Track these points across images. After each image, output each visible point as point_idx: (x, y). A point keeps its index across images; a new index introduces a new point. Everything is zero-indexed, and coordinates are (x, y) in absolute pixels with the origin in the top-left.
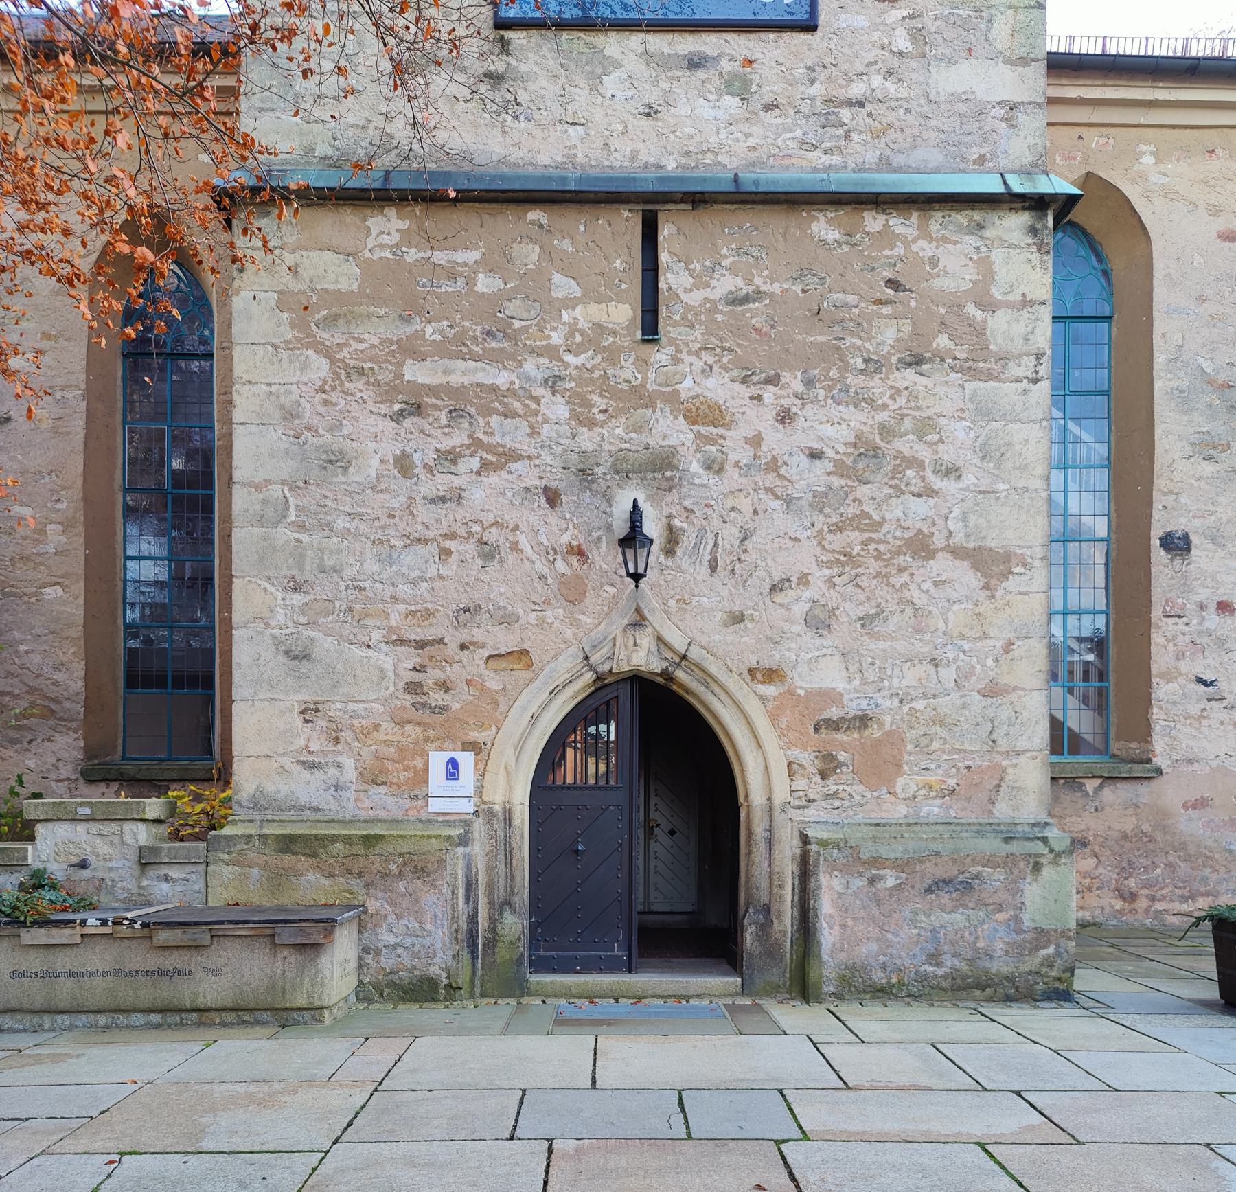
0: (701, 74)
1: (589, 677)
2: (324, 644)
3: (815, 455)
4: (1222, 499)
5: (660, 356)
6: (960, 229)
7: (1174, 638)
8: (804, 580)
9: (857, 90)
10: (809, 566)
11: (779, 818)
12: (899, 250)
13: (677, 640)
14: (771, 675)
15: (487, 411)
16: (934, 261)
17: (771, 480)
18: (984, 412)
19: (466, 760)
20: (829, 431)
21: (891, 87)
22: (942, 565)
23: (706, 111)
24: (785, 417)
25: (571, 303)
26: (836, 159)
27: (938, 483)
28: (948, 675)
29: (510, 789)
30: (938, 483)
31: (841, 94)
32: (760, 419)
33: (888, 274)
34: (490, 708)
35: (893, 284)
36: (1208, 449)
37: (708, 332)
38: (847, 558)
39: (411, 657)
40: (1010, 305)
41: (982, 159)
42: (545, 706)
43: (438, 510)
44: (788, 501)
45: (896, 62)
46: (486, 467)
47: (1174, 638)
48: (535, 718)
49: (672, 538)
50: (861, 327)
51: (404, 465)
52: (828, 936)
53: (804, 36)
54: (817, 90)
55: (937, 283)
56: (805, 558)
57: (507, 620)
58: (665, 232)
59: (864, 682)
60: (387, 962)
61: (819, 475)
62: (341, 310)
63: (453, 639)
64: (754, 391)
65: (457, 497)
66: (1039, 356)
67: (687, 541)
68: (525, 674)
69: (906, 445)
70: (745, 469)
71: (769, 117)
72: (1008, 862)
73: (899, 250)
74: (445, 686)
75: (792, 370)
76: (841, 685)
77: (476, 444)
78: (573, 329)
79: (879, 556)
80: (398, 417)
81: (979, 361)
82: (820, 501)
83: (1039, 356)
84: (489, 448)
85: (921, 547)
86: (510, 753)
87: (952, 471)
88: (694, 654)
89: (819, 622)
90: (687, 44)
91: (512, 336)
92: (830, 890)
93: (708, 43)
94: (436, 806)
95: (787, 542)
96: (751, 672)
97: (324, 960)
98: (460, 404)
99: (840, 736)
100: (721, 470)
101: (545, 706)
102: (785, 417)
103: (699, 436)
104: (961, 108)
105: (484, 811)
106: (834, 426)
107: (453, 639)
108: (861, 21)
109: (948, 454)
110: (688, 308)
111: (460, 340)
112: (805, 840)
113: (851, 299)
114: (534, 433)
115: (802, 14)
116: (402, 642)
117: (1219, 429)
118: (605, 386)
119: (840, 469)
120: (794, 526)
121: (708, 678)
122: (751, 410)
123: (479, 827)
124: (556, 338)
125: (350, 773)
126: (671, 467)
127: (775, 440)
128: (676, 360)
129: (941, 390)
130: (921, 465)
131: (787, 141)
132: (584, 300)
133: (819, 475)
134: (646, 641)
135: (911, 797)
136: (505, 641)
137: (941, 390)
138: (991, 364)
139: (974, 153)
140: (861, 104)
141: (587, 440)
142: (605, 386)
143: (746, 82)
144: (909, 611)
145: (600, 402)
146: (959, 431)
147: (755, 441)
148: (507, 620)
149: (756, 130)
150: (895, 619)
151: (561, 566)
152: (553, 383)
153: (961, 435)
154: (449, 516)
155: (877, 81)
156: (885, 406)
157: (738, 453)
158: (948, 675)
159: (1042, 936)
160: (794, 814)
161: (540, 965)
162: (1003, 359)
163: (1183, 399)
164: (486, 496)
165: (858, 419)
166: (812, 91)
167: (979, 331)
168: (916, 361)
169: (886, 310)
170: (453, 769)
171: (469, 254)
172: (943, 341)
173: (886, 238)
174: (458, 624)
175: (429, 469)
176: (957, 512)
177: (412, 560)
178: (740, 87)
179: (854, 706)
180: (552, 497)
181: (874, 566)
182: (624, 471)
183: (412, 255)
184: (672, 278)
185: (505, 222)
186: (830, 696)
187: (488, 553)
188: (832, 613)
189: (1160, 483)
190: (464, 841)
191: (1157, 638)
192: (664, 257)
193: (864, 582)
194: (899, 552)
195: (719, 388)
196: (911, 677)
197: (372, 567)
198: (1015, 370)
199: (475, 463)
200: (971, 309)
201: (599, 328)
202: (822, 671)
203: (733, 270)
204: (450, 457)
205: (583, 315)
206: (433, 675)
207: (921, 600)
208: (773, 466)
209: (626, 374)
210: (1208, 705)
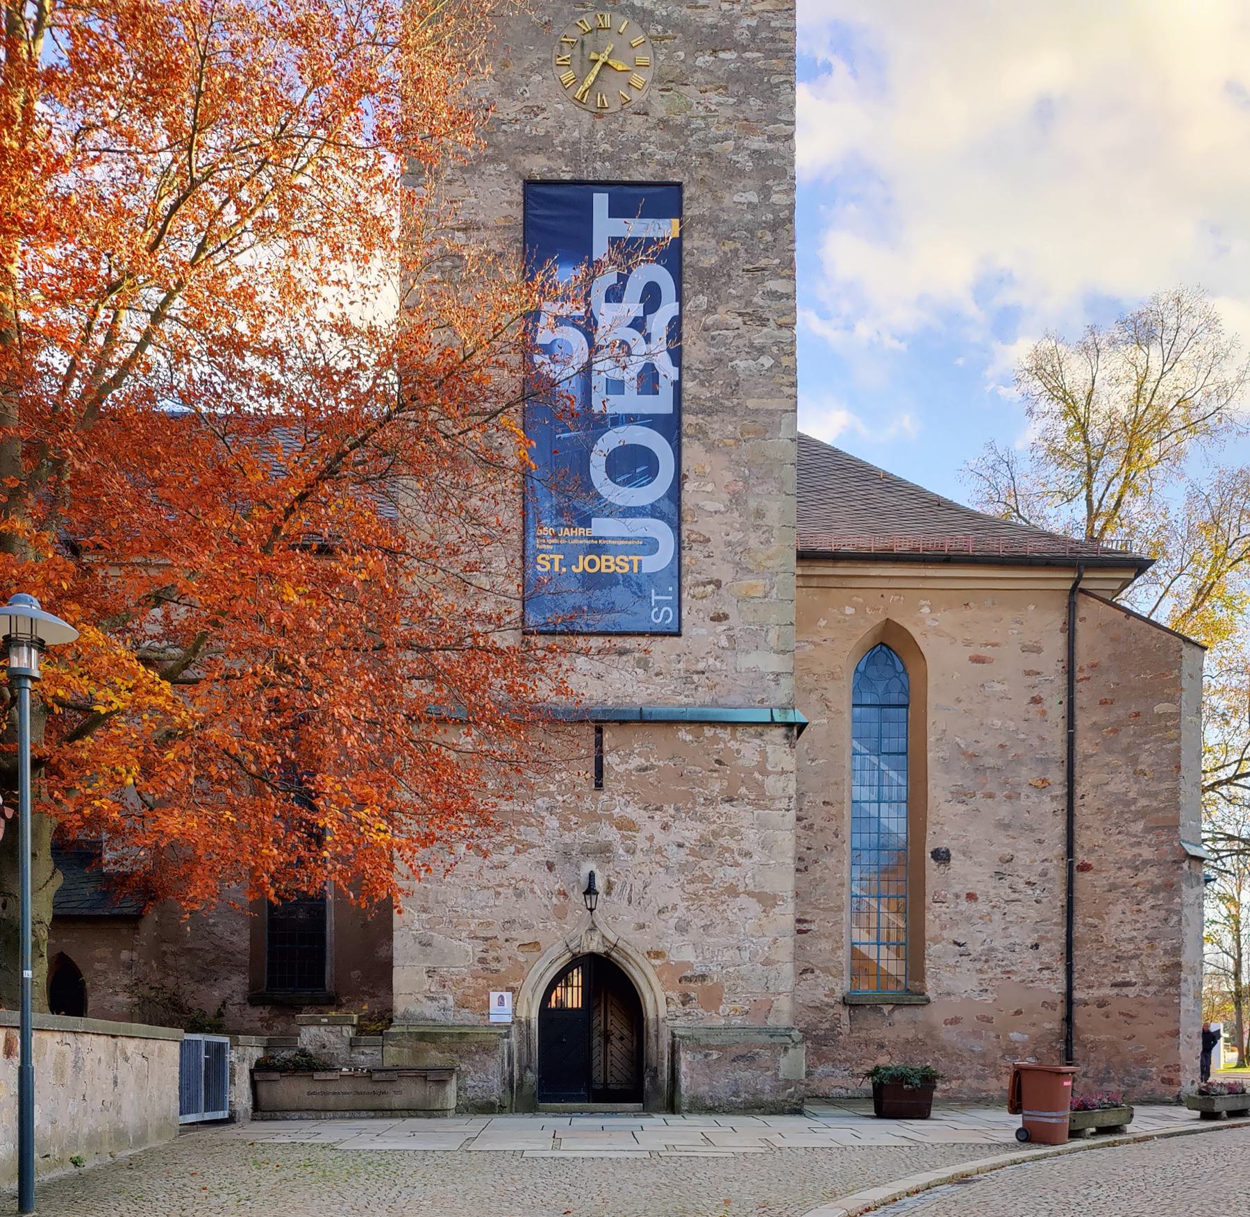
0: (624, 658)
1: (569, 955)
2: (438, 938)
3: (680, 846)
4: (970, 828)
5: (604, 797)
6: (752, 736)
7: (939, 916)
8: (675, 907)
9: (701, 666)
11: (661, 1025)
12: (722, 746)
13: (612, 937)
14: (658, 955)
16: (738, 751)
17: (658, 858)
18: (763, 825)
19: (508, 996)
20: (687, 833)
21: (718, 664)
22: (743, 900)
26: (691, 700)
27: (740, 860)
28: (746, 955)
29: (529, 1011)
30: (740, 860)
31: (694, 668)
32: (654, 828)
33: (716, 757)
34: (520, 971)
35: (717, 761)
37: (627, 785)
38: (696, 897)
40: (776, 773)
41: (762, 701)
42: (547, 969)
43: (494, 873)
44: (667, 868)
45: (721, 651)
46: (518, 851)
47: (939, 916)
48: (542, 976)
49: (610, 887)
50: (703, 783)
52: (684, 1082)
53: (675, 639)
54: (681, 666)
55: (740, 762)
56: (675, 896)
57: (529, 927)
58: (607, 736)
59: (704, 958)
60: (470, 1094)
61: (682, 855)
63: (502, 936)
64: (650, 814)
66: (790, 798)
67: (617, 888)
68: (537, 954)
69: (725, 841)
70: (646, 852)
72: (772, 1047)
73: (722, 746)
74: (498, 960)
75: (669, 803)
76: (692, 960)
79: (712, 896)
81: (761, 800)
82: (683, 868)
83: (790, 798)
84: (519, 842)
85: (732, 891)
86: (530, 993)
87: (748, 854)
88: (620, 944)
89: (682, 928)
90: (619, 642)
92: (686, 1059)
93: (630, 643)
94: (493, 1019)
95: (667, 890)
97: (448, 1088)
99: (691, 985)
100: (634, 853)
101: (547, 969)
102: (665, 827)
103: (623, 836)
104: (753, 675)
105: (517, 1021)
106: (690, 832)
107: (502, 936)
109: (745, 846)
110: (618, 773)
112: (674, 1036)
113: (698, 769)
114: (542, 834)
115: (675, 630)
117: (967, 782)
118: (576, 811)
119: (692, 852)
120: (668, 880)
121: (627, 956)
122: (649, 823)
123: (514, 1029)
124: (553, 788)
125: (451, 1002)
126: (609, 851)
127: (661, 838)
128: (612, 799)
129: (742, 814)
131: (668, 691)
133: (682, 855)
134: (597, 938)
137: (742, 814)
138: (767, 802)
139: (759, 698)
140: (703, 673)
141: (568, 837)
142: (576, 811)
143: (647, 663)
144: (726, 923)
145: (575, 819)
146: (751, 834)
148: (529, 927)
151: (555, 900)
152: (551, 810)
154: (500, 875)
155: (711, 661)
156: (714, 822)
157: (643, 844)
158: (746, 955)
159: (788, 1083)
160: (669, 1023)
161: (544, 1099)
162: (772, 799)
163: (946, 764)
164: (519, 866)
165: (701, 827)
166: (679, 666)
167: (761, 786)
169: (715, 775)
172: (743, 790)
173: (715, 739)
174: (504, 929)
176: (750, 874)
177: (481, 897)
178: (644, 664)
179: (699, 970)
180: (550, 866)
181: (709, 900)
182: (586, 852)
184: (609, 759)
186: (689, 965)
187: (519, 894)
189: (931, 817)
190: (507, 1036)
191: (929, 916)
193: (704, 908)
194: (722, 893)
195: (633, 812)
196: (727, 956)
197: (461, 901)
198: (778, 805)
199: (512, 849)
200: (756, 775)
202: (684, 953)
203: (640, 755)
206: (492, 954)
208: (659, 851)
209: (587, 805)
210: (960, 959)
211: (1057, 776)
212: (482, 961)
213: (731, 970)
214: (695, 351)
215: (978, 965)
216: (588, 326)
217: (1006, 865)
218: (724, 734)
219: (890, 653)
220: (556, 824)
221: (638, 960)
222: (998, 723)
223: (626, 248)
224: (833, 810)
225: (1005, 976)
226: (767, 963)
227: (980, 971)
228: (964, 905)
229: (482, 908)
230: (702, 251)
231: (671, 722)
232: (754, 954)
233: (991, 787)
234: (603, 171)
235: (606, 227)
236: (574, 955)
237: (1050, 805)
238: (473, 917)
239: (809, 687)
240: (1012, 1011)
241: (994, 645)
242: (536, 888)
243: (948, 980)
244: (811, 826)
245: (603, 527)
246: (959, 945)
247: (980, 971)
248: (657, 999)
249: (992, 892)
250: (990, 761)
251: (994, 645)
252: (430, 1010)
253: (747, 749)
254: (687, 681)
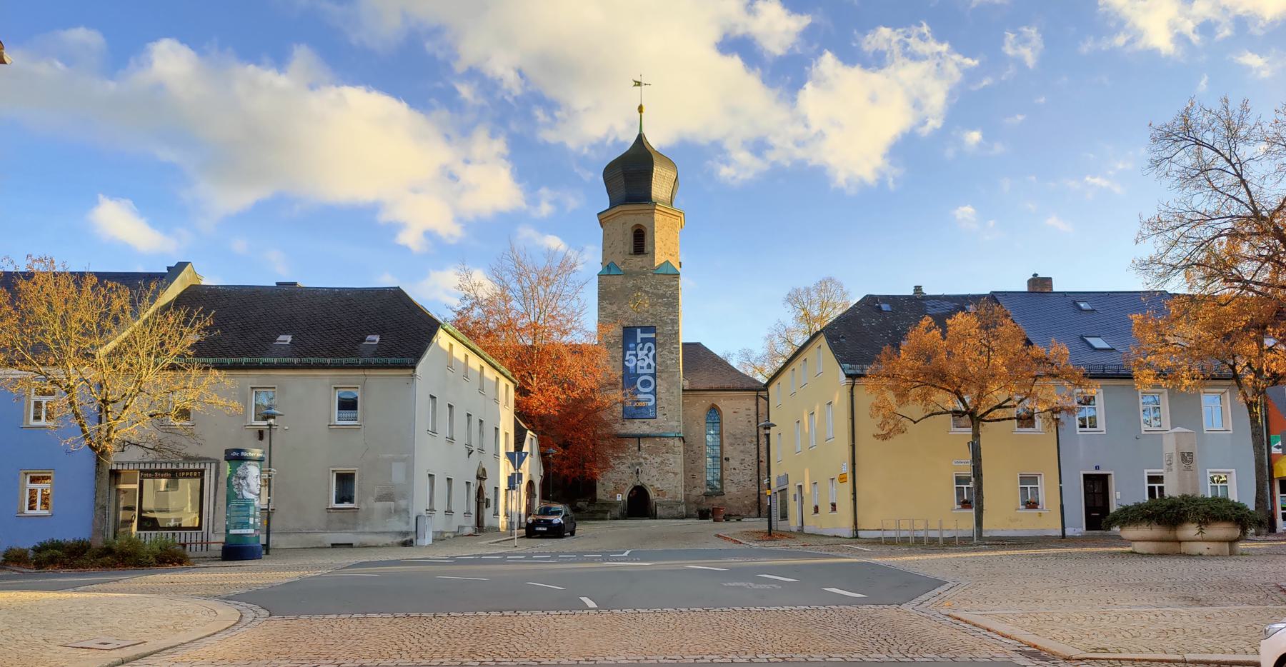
36: (731, 445)
81: (674, 453)
95: (654, 472)
99: (659, 491)
106: (659, 460)
135: (667, 498)
211: (755, 439)
214: (658, 360)
216: (636, 355)
219: (714, 409)
223: (644, 341)
230: (660, 339)
234: (639, 324)
235: (640, 335)
237: (753, 446)
243: (729, 489)
245: (640, 396)
248: (652, 495)
253: (671, 442)
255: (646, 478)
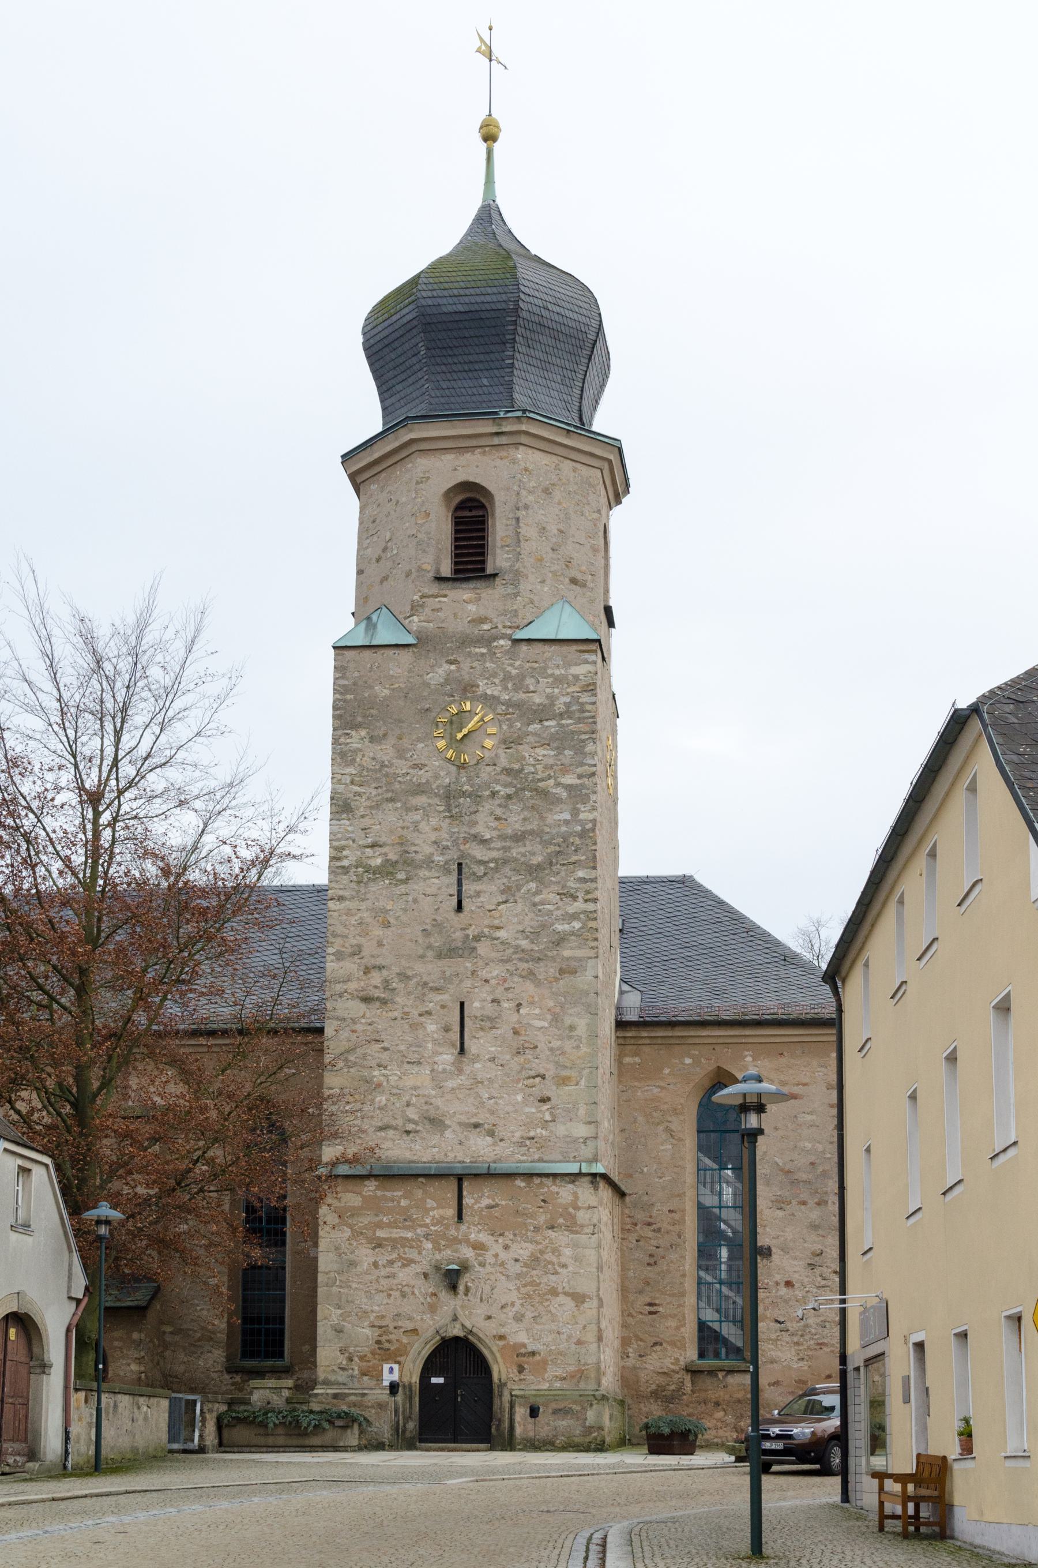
1: (438, 1338)
3: (517, 1260)
4: (787, 1229)
5: (463, 1227)
8: (513, 1304)
10: (515, 1299)
13: (468, 1325)
14: (502, 1337)
15: (404, 1246)
16: (558, 1193)
18: (576, 1245)
19: (396, 1367)
20: (522, 1252)
23: (480, 1141)
24: (506, 1247)
25: (433, 1209)
30: (560, 1270)
32: (498, 1248)
33: (542, 1198)
35: (544, 1201)
39: (377, 1332)
44: (508, 1276)
46: (404, 1266)
48: (419, 1353)
51: (375, 1265)
55: (560, 1201)
56: (514, 1296)
58: (465, 1184)
61: (518, 1268)
62: (355, 1212)
65: (393, 1276)
67: (472, 1291)
68: (416, 1337)
69: (549, 1256)
70: (493, 1265)
71: (501, 1144)
73: (546, 1189)
74: (388, 1341)
75: (509, 1230)
76: (526, 1341)
77: (401, 1257)
78: (433, 1218)
79: (539, 1295)
80: (374, 1249)
82: (519, 1276)
87: (565, 1266)
88: (475, 1330)
89: (519, 1318)
91: (413, 1221)
95: (507, 1291)
96: (494, 1336)
98: (395, 1243)
100: (484, 1266)
102: (506, 1247)
104: (568, 1139)
106: (523, 1250)
108: (533, 1110)
109: (563, 1260)
111: (395, 1222)
114: (420, 1253)
116: (374, 1326)
118: (444, 1236)
119: (526, 1265)
121: (479, 1339)
122: (495, 1246)
124: (428, 1221)
127: (503, 1255)
128: (469, 1228)
130: (553, 1264)
132: (437, 1208)
133: (518, 1268)
134: (458, 1326)
136: (410, 1326)
138: (578, 1228)
141: (438, 1256)
145: (443, 1243)
146: (567, 1252)
147: (496, 1256)
149: (497, 1148)
150: (545, 1317)
152: (426, 1237)
153: (568, 1253)
162: (582, 1226)
164: (405, 1275)
165: (531, 1247)
167: (574, 1217)
168: (552, 1227)
170: (391, 1370)
171: (398, 1195)
172: (561, 1220)
175: (384, 1266)
177: (378, 1298)
179: (530, 1349)
180: (426, 1275)
181: (537, 1299)
183: (379, 1193)
184: (467, 1200)
185: (410, 1185)
186: (524, 1346)
187: (404, 1295)
188: (523, 1316)
192: (465, 1193)
195: (484, 1237)
199: (400, 1264)
200: (571, 1210)
201: (443, 1218)
202: (520, 1336)
203: (488, 1197)
204: (391, 1263)
205: (436, 1213)
207: (554, 1311)
208: (502, 1264)
212: (378, 1342)
213: (553, 1348)
215: (795, 1339)
217: (817, 1258)
218: (548, 1182)
220: (430, 1246)
221: (487, 1341)
222: (808, 1145)
224: (676, 1216)
225: (818, 1347)
226: (579, 1342)
227: (797, 1344)
228: (783, 1291)
229: (378, 1306)
231: (510, 1176)
232: (570, 1337)
233: (804, 1196)
236: (443, 1338)
238: (372, 1311)
239: (657, 1120)
240: (824, 1376)
241: (804, 1085)
242: (416, 1292)
244: (659, 1230)
246: (779, 1322)
247: (797, 1344)
248: (501, 1369)
249: (806, 1280)
250: (804, 1176)
251: (804, 1085)
252: (341, 1377)
253: (565, 1192)
254: (522, 1144)
255: (481, 1310)
